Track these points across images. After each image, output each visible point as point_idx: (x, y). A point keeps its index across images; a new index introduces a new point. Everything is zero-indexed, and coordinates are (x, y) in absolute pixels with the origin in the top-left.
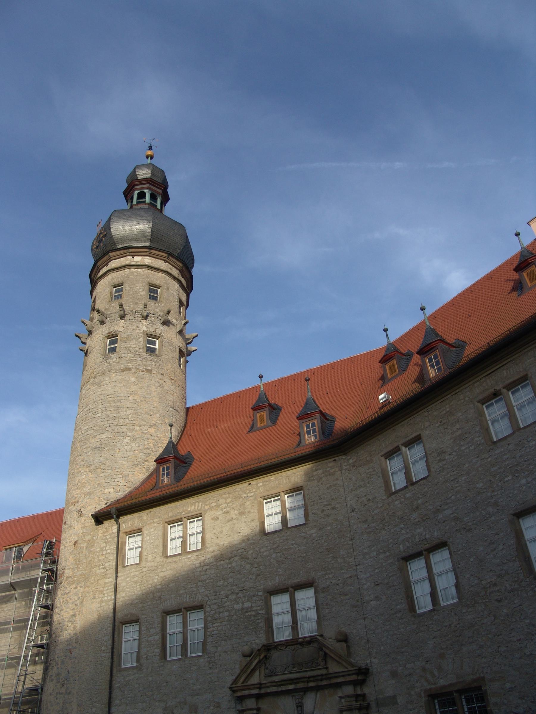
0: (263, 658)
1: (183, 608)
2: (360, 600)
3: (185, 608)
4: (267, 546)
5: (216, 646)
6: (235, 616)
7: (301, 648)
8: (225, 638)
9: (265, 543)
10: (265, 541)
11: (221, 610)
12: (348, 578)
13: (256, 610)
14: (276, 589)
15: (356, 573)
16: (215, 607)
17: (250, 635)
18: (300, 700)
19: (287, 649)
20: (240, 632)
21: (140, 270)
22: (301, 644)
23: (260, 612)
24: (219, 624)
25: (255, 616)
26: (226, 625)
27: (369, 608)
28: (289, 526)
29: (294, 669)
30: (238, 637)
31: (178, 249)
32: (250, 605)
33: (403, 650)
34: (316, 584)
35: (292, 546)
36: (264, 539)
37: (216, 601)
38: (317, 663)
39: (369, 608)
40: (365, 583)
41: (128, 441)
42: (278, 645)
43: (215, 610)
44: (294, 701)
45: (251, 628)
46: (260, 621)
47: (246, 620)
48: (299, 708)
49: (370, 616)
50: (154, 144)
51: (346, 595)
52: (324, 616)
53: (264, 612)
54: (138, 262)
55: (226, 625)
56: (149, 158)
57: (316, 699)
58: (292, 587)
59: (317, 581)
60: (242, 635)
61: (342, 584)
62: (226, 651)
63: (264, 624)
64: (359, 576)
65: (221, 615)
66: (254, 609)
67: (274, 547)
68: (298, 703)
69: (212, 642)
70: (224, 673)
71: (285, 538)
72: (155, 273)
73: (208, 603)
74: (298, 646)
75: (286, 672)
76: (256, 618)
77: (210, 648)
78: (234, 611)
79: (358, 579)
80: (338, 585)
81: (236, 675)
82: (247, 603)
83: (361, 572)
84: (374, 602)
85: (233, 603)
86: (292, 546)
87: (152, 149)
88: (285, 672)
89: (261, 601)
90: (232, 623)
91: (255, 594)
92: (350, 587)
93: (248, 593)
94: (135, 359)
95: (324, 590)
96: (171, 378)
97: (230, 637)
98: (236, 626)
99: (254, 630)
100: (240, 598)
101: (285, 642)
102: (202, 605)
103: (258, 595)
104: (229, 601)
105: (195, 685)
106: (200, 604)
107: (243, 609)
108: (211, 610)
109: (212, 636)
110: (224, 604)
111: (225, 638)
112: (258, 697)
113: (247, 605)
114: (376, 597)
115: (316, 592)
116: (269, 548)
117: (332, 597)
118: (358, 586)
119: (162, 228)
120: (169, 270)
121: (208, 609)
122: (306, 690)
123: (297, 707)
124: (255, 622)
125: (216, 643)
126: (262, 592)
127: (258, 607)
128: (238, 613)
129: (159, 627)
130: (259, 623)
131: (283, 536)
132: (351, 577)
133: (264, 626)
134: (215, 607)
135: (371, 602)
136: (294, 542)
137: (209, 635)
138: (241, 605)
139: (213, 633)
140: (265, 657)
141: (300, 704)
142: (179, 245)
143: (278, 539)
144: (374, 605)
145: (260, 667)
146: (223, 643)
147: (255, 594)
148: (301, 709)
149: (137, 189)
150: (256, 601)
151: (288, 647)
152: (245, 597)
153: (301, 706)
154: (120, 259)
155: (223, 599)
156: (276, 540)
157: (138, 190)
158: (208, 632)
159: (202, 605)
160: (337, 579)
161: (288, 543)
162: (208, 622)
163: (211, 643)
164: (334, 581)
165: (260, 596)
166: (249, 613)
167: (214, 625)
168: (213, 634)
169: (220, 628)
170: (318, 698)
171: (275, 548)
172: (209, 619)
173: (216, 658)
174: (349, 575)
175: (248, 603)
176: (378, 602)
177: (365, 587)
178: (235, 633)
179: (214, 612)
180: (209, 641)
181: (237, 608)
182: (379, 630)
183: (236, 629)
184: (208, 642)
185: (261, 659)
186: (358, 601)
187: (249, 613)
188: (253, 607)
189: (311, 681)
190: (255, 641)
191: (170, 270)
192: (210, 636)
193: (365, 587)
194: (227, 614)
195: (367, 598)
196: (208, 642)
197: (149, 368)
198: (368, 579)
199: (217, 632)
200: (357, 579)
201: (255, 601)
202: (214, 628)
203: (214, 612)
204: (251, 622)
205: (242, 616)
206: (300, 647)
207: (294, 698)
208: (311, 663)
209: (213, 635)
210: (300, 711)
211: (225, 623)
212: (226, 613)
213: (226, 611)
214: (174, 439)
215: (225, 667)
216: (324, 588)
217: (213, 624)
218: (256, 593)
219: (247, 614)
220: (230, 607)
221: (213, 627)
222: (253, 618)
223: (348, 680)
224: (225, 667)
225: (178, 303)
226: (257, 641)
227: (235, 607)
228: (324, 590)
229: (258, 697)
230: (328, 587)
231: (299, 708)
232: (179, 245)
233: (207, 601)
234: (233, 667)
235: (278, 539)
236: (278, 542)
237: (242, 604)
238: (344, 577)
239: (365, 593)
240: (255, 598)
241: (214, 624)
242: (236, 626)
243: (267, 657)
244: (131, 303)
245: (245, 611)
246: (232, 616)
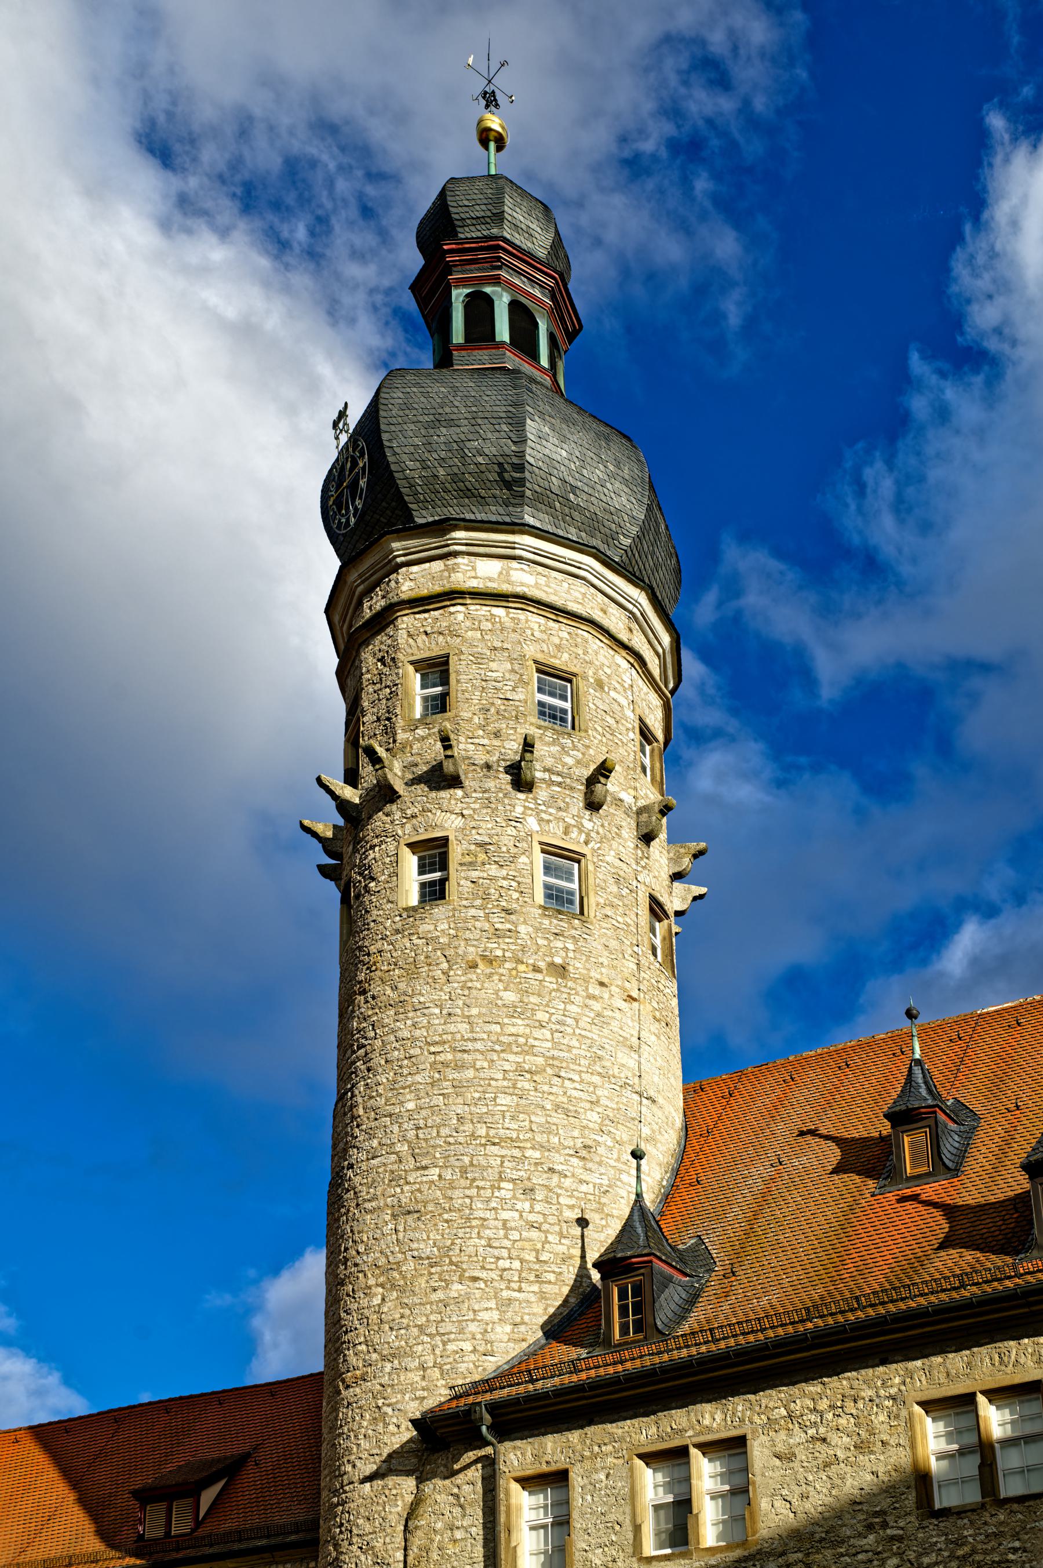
4: (940, 1550)
9: (935, 1540)
10: (934, 1533)
21: (500, 612)
28: (1003, 1495)
31: (624, 534)
35: (1011, 1557)
36: (931, 1527)
41: (509, 1194)
50: (502, 84)
54: (490, 579)
56: (492, 145)
67: (960, 1553)
71: (991, 1529)
72: (551, 624)
86: (1011, 1557)
87: (497, 105)
94: (508, 926)
96: (629, 996)
116: (946, 1554)
119: (564, 453)
120: (598, 616)
131: (985, 1523)
136: (1017, 1544)
142: (626, 518)
143: (971, 1532)
149: (462, 282)
154: (427, 565)
156: (966, 1533)
157: (465, 286)
161: (1000, 1544)
171: (964, 1556)
191: (601, 614)
197: (558, 960)
214: (650, 1201)
225: (638, 737)
232: (626, 518)
235: (971, 1532)
236: (970, 1539)
244: (481, 733)
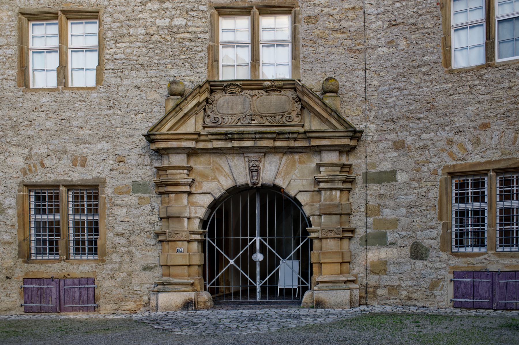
0: (202, 102)
1: (59, 12)
2: (363, 43)
3: (63, 12)
5: (120, 77)
6: (156, 36)
7: (266, 95)
8: (137, 66)
11: (133, 23)
12: (349, 9)
13: (195, 32)
14: (231, 6)
15: (362, 4)
16: (121, 17)
17: (181, 67)
18: (257, 164)
19: (242, 93)
20: (164, 61)
22: (267, 89)
23: (199, 36)
24: (127, 44)
25: (191, 40)
26: (139, 47)
27: (375, 56)
29: (253, 122)
30: (161, 68)
32: (184, 22)
33: (421, 115)
34: (298, 9)
37: (123, 9)
38: (289, 118)
39: (375, 56)
40: (374, 20)
42: (230, 85)
43: (121, 22)
44: (247, 164)
45: (184, 57)
46: (199, 49)
47: (175, 44)
48: (255, 174)
49: (374, 67)
51: (343, 33)
52: (304, 57)
53: (208, 38)
55: (139, 47)
57: (280, 164)
58: (257, 7)
59: (300, 4)
60: (167, 65)
61: (338, 16)
62: (139, 85)
63: (206, 54)
64: (366, 10)
65: (132, 31)
66: (190, 30)
68: (254, 167)
69: (113, 70)
70: (133, 116)
73: (109, 9)
74: (262, 91)
75: (239, 124)
76: (193, 44)
77: (110, 78)
78: (155, 28)
79: (364, 12)
80: (332, 16)
81: (155, 121)
82: (179, 19)
83: (370, 4)
84: (385, 48)
85: (153, 15)
88: (238, 124)
89: (204, 20)
90: (151, 46)
91: (194, 7)
92: (351, 23)
93: (182, 4)
95: (310, 20)
97: (146, 66)
98: (157, 51)
99: (189, 61)
100: (167, 9)
101: (242, 83)
102: (98, 12)
103: (198, 10)
104: (146, 12)
105: (81, 128)
106: (95, 8)
107: (170, 27)
108: (114, 22)
109: (115, 61)
110: (137, 15)
111: (137, 66)
112: (192, 153)
113: (179, 22)
114: (389, 43)
115: (294, 22)
117: (321, 32)
118: (363, 24)
121: (107, 19)
122: (267, 151)
123: (252, 172)
124: (191, 49)
125: (122, 72)
126: (206, 6)
127: (198, 27)
128: (161, 33)
129: (14, 36)
130: (198, 52)
132: (354, 9)
133: (207, 58)
134: (121, 17)
135: (379, 49)
137: (108, 59)
138: (168, 20)
139: (117, 57)
140: (207, 100)
141: (256, 168)
144: (383, 53)
145: (197, 114)
146: (133, 73)
147: (194, 7)
148: (258, 174)
150: (195, 19)
151: (244, 91)
152: (176, 10)
153: (257, 171)
155: (136, 8)
158: (107, 54)
159: (98, 12)
160: (333, 8)
162: (107, 39)
163: (111, 71)
164: (326, 10)
165: (202, 11)
166: (182, 35)
167: (118, 45)
168: (115, 57)
169: (129, 51)
170: (282, 164)
172: (109, 34)
173: (120, 94)
174: (352, 6)
175: (181, 19)
176: (392, 50)
177: (373, 26)
178: (156, 61)
179: (119, 24)
180: (108, 67)
181: (161, 24)
182: (386, 87)
183: (158, 56)
184: (106, 70)
185: (201, 101)
186: (359, 44)
187: (182, 35)
188: (190, 27)
189: (279, 139)
190: (188, 78)
192: (110, 61)
193: (373, 26)
194: (142, 31)
195: (374, 42)
196: (106, 70)
198: (380, 16)
199: (123, 56)
200: (362, 13)
201: (192, 18)
202: (118, 50)
203: (119, 24)
204: (184, 49)
205: (169, 38)
206: (265, 93)
207: (246, 159)
208: (281, 116)
209: (115, 59)
210: (256, 177)
211: (138, 44)
212: (140, 29)
213: (140, 27)
215: (137, 108)
216: (309, 17)
217: (116, 42)
218: (196, 6)
219: (178, 36)
220: (148, 20)
221: (116, 47)
222: (187, 43)
223: (336, 143)
224: (137, 108)
226: (192, 78)
227: (157, 22)
228: (310, 20)
229: (192, 153)
230: (316, 17)
231: (253, 173)
233: (105, 7)
234: (150, 110)
237: (169, 20)
238: (343, 7)
239: (372, 35)
240: (194, 13)
241: (119, 43)
242: (157, 51)
243: (210, 100)
245: (175, 30)
246: (152, 35)
